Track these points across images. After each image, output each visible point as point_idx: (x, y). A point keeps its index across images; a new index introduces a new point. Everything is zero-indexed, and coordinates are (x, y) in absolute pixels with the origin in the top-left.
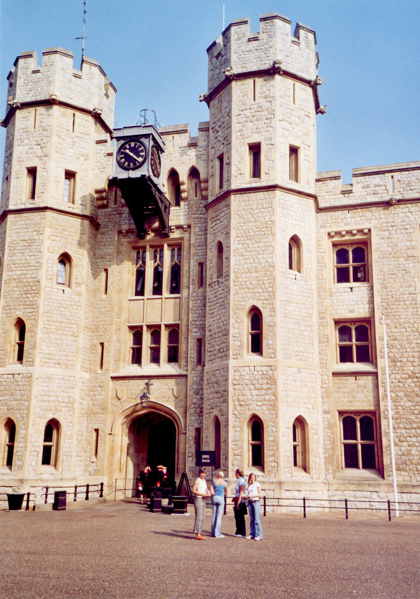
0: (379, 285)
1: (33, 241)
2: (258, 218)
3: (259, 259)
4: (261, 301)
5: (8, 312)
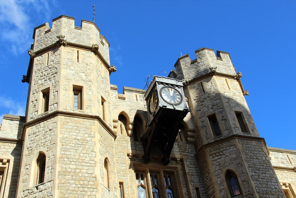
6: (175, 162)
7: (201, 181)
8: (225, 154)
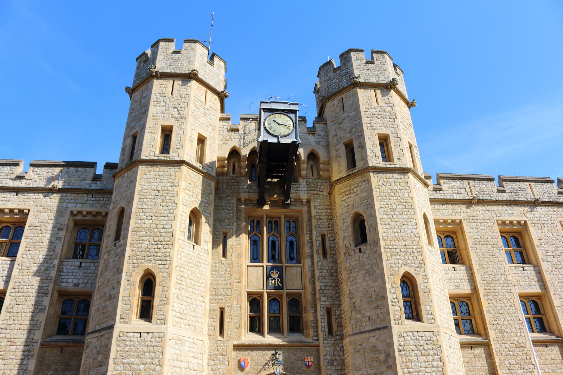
0: (478, 266)
1: (167, 192)
2: (397, 194)
3: (404, 229)
4: (413, 268)
5: (135, 262)
6: (300, 204)
7: (330, 226)
8: (355, 193)
